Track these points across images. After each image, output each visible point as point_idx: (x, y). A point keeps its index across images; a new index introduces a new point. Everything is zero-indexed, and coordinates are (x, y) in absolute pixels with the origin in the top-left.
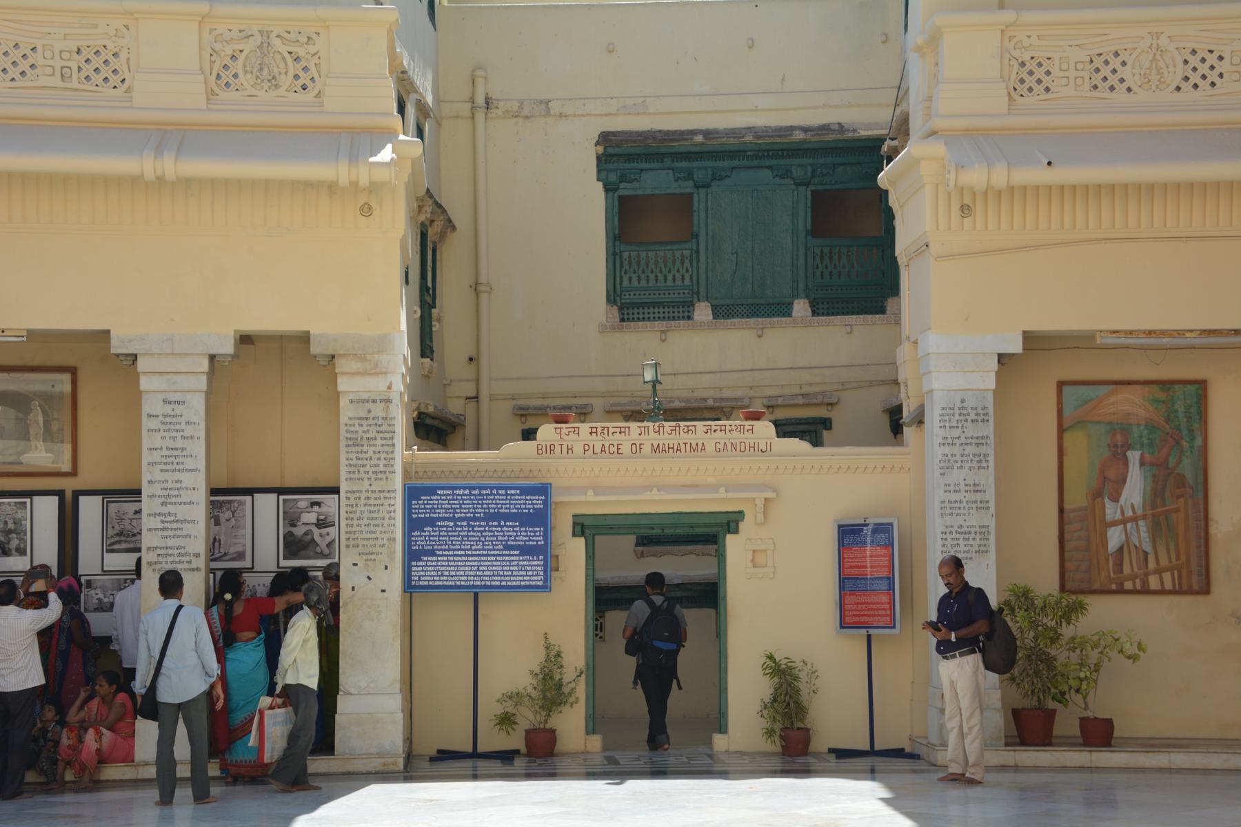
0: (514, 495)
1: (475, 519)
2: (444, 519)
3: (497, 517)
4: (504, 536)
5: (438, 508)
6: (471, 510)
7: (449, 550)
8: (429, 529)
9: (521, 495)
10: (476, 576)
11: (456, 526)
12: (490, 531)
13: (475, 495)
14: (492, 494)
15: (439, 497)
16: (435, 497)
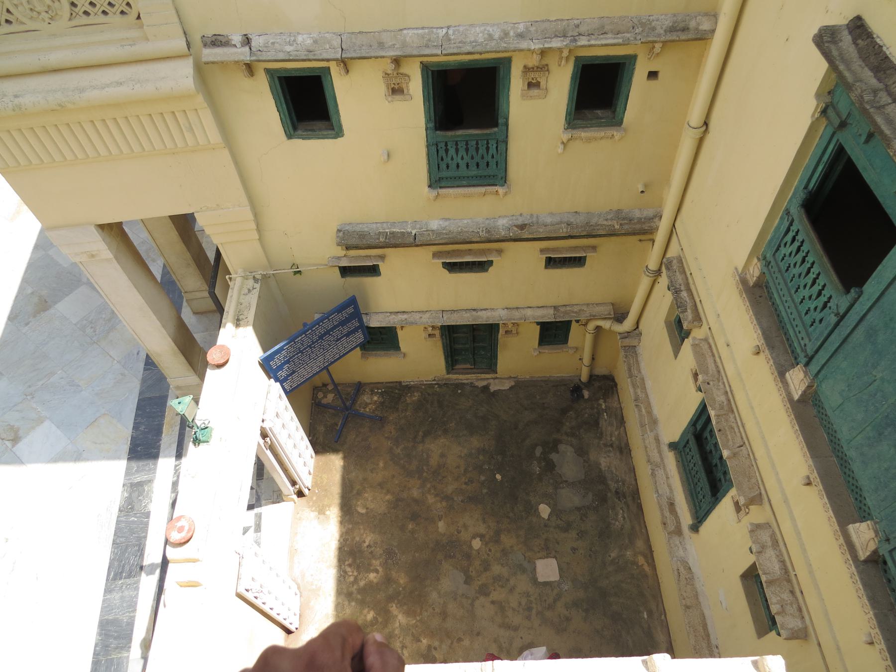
0: (335, 316)
1: (313, 343)
2: (294, 356)
3: (327, 333)
4: (334, 337)
5: (288, 354)
6: (310, 341)
7: (303, 365)
8: (286, 366)
9: (338, 314)
10: (324, 363)
11: (303, 353)
12: (324, 342)
13: (309, 334)
14: (319, 326)
15: (286, 350)
16: (284, 351)
